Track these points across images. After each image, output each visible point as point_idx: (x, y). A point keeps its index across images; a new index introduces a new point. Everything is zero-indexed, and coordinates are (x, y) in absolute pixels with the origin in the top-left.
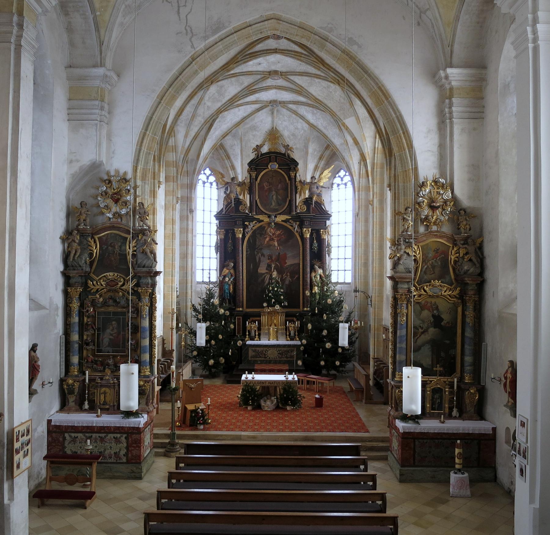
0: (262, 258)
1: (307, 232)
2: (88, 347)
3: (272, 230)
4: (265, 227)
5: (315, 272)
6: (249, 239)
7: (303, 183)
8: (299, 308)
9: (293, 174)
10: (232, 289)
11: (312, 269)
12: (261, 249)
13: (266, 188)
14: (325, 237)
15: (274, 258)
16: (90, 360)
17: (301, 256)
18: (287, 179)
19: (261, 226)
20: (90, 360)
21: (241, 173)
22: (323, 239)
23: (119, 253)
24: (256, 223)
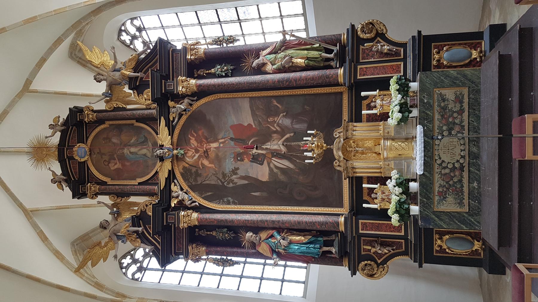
0: (241, 173)
1: (185, 83)
3: (190, 154)
4: (184, 168)
5: (264, 64)
6: (205, 198)
7: (109, 95)
8: (341, 93)
9: (92, 117)
10: (298, 238)
11: (260, 70)
12: (224, 175)
13: (118, 166)
14: (202, 48)
15: (239, 150)
17: (235, 95)
18: (102, 127)
19: (182, 174)
21: (96, 210)
22: (205, 53)
24: (175, 185)
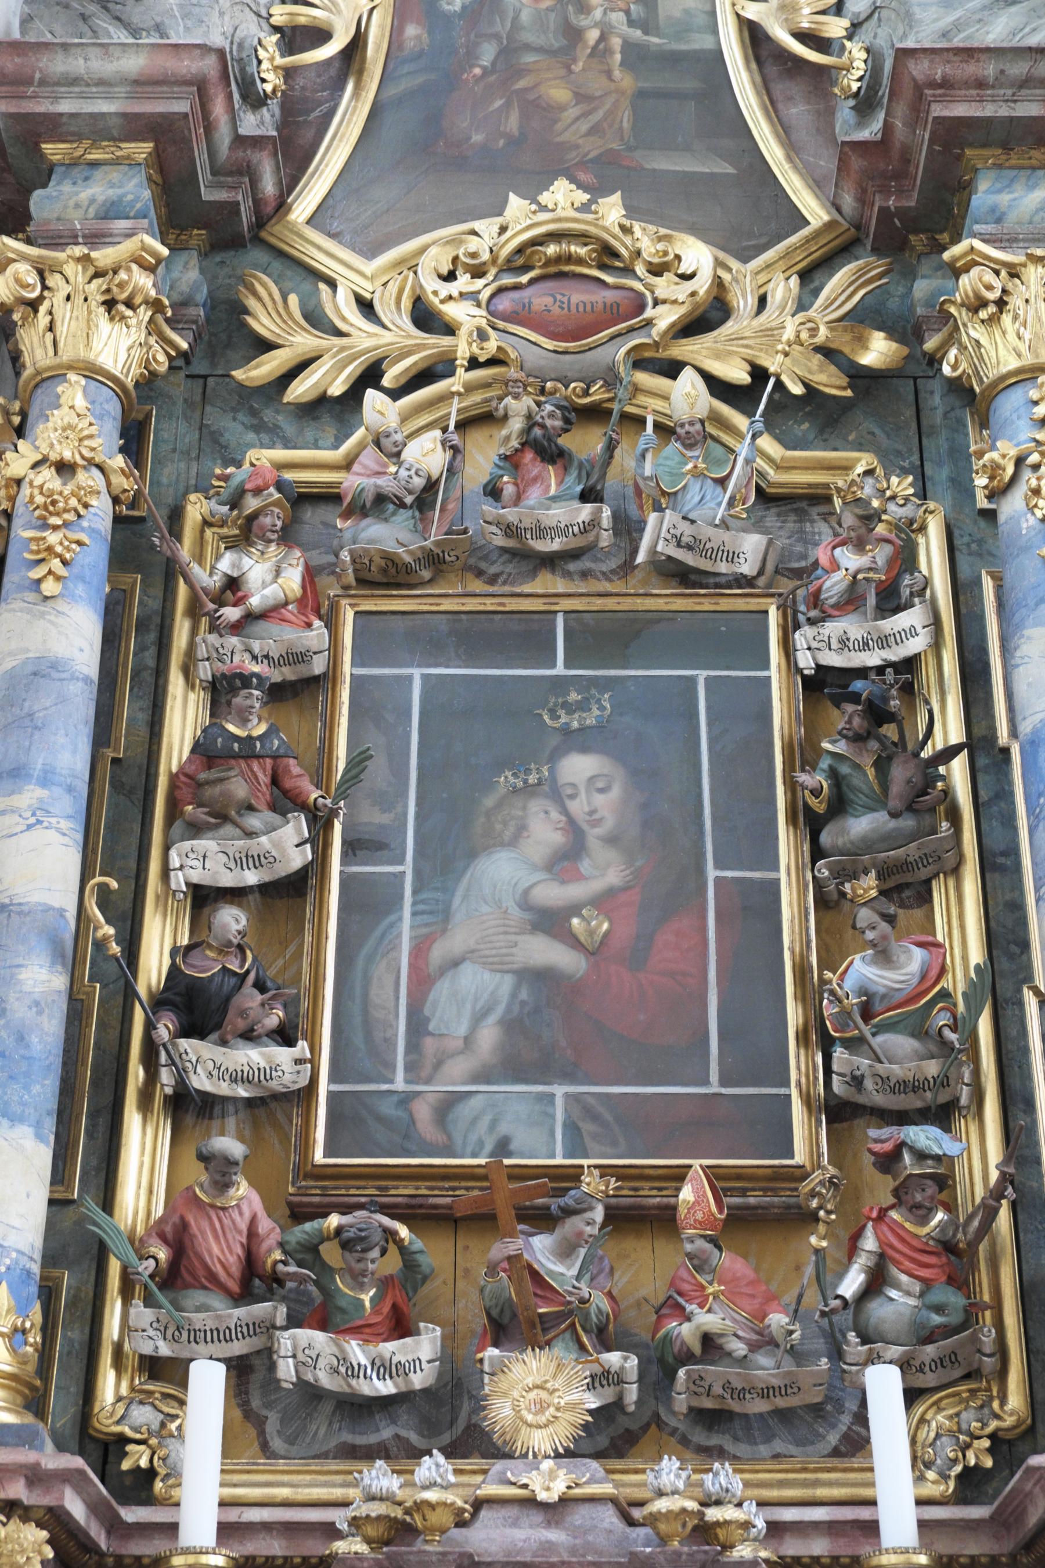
2: (211, 1065)
16: (220, 1250)
20: (220, 1250)
23: (628, 46)
